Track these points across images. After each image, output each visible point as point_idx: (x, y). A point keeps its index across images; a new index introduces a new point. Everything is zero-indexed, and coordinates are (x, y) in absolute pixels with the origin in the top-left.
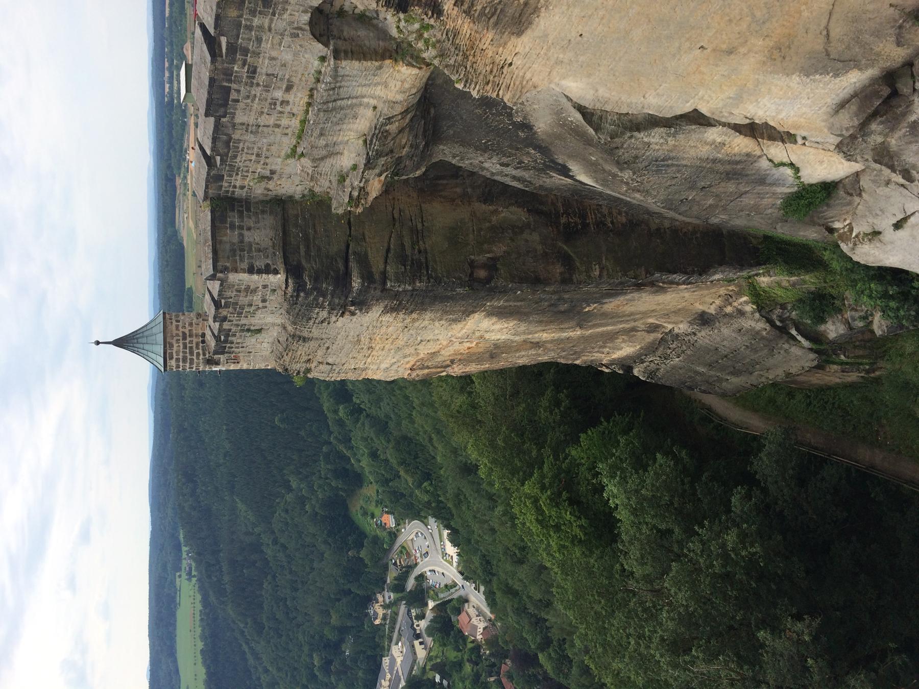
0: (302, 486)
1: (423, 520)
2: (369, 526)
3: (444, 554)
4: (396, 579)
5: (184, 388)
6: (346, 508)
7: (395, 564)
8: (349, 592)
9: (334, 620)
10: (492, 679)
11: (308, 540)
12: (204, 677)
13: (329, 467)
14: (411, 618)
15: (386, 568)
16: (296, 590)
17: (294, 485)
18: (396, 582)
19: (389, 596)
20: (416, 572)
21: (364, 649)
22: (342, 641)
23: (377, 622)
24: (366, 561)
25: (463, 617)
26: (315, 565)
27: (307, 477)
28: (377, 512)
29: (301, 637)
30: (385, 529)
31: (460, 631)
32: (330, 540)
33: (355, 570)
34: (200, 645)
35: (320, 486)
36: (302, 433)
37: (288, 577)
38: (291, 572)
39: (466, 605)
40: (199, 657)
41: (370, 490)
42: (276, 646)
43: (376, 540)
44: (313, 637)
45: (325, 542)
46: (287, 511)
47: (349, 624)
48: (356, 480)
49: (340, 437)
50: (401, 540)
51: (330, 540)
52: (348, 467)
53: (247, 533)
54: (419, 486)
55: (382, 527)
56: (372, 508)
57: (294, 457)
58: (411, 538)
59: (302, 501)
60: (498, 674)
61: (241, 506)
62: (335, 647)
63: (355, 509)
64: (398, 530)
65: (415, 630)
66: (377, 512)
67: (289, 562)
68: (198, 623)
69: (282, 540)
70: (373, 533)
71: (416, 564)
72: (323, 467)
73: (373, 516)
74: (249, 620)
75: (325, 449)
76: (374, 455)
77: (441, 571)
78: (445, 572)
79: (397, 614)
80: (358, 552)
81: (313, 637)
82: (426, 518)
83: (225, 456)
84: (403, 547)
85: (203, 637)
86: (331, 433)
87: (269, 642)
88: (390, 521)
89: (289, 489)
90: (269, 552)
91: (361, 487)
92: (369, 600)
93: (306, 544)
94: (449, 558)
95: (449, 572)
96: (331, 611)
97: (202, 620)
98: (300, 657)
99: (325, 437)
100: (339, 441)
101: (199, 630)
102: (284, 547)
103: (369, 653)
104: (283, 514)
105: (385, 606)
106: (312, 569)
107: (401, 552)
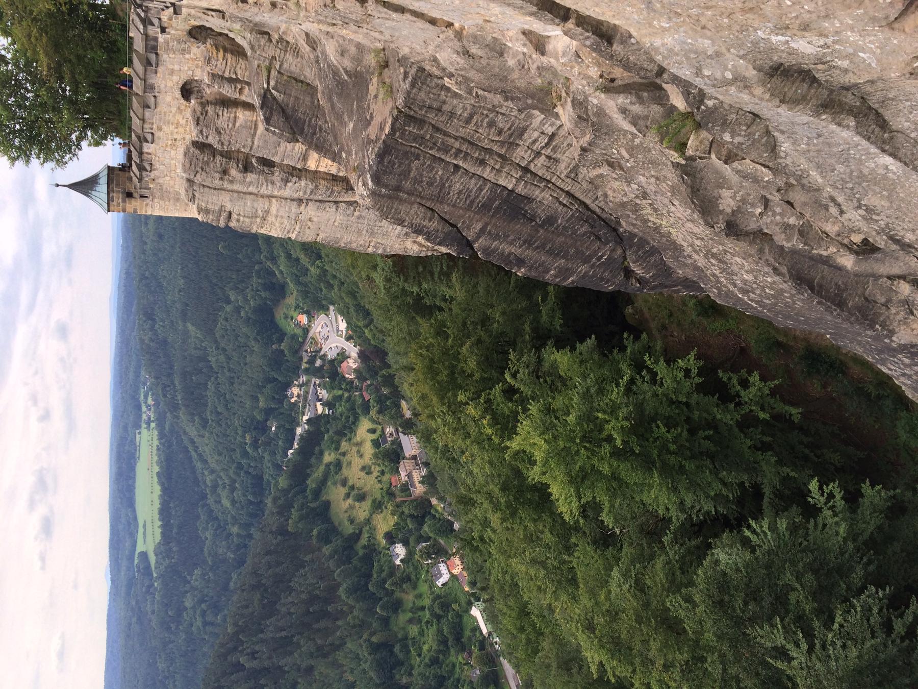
0: (239, 297)
1: (326, 310)
2: (289, 327)
3: (338, 331)
4: (306, 363)
5: (146, 243)
6: (273, 316)
7: (306, 351)
8: (275, 380)
9: (261, 404)
10: (357, 394)
11: (242, 340)
12: (159, 493)
13: (260, 281)
14: (316, 389)
15: (301, 359)
16: (232, 384)
17: (232, 298)
18: (307, 366)
19: (303, 379)
20: (322, 353)
21: (283, 423)
22: (266, 420)
23: (293, 401)
24: (286, 352)
25: (344, 365)
26: (248, 359)
27: (243, 291)
28: (295, 315)
29: (236, 423)
30: (300, 327)
31: (344, 377)
32: (259, 338)
33: (277, 361)
34: (156, 469)
35: (252, 298)
36: (240, 256)
37: (228, 374)
38: (229, 371)
39: (348, 360)
40: (156, 479)
41: (291, 300)
42: (217, 435)
43: (294, 337)
44: (245, 421)
45: (255, 339)
46: (226, 320)
47: (272, 406)
48: (278, 291)
49: (268, 255)
50: (311, 334)
51: (259, 338)
52: (274, 281)
53: (196, 348)
54: (313, 264)
55: (298, 325)
56: (292, 313)
57: (234, 276)
58: (318, 330)
59: (238, 310)
60: (361, 390)
61: (190, 326)
62: (262, 428)
63: (279, 315)
64: (309, 326)
65: (318, 396)
66: (295, 315)
67: (228, 363)
68: (155, 452)
69: (222, 345)
70: (292, 333)
71: (321, 349)
72: (255, 281)
73: (292, 318)
74: (196, 418)
75: (256, 267)
76: (289, 256)
77: (335, 345)
78: (338, 345)
79: (307, 393)
80: (280, 346)
81: (245, 421)
82: (328, 309)
83: (180, 291)
84: (313, 338)
85: (159, 463)
86: (261, 253)
87: (212, 433)
88: (304, 319)
89: (228, 302)
90: (212, 359)
91: (284, 298)
92: (289, 385)
93: (242, 345)
94: (340, 333)
95: (337, 342)
96: (259, 395)
97: (158, 449)
98: (235, 439)
99: (257, 257)
100: (267, 259)
101: (156, 458)
102: (224, 350)
103: (287, 426)
104: (224, 323)
105: (300, 386)
106: (245, 364)
107: (311, 343)
